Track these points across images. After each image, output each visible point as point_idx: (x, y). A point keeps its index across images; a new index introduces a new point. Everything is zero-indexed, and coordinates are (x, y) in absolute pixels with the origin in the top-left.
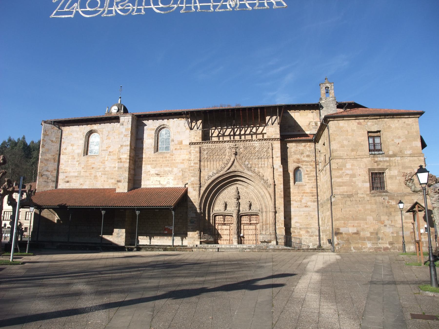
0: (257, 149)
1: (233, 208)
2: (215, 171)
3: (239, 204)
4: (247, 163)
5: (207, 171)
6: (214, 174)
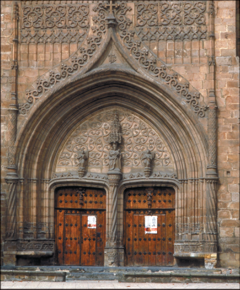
0: (172, 14)
1: (105, 170)
2: (58, 71)
3: (122, 159)
4: (144, 49)
5: (35, 68)
6: (54, 78)
